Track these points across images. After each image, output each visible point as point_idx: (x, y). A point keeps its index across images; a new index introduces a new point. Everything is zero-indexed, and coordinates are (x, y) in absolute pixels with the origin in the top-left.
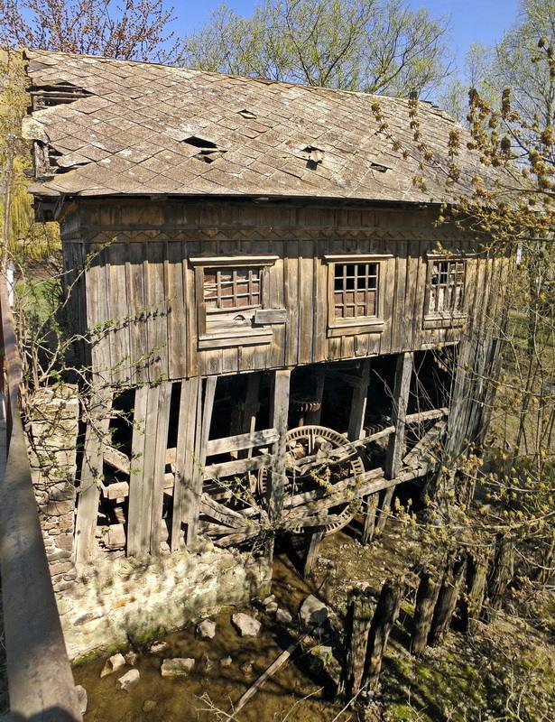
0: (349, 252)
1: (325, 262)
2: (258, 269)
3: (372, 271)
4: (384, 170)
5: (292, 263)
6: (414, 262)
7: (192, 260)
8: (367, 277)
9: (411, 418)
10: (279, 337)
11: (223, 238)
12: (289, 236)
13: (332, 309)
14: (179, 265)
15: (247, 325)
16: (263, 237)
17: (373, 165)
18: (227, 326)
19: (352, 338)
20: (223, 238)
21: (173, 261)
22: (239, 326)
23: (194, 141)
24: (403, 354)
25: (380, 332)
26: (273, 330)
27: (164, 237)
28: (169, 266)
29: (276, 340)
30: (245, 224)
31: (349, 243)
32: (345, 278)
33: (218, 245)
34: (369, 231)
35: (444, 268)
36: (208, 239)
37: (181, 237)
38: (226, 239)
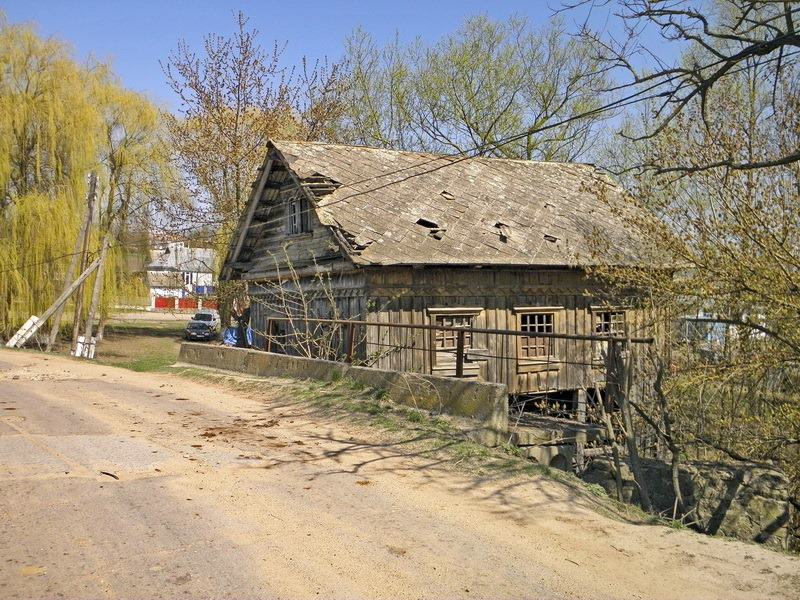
0: (530, 304)
1: (514, 313)
2: (468, 318)
3: (548, 321)
4: (554, 241)
5: (492, 313)
6: (580, 313)
7: (430, 309)
8: (544, 325)
9: (589, 452)
11: (447, 294)
13: (520, 350)
14: (420, 313)
17: (546, 236)
19: (535, 375)
20: (447, 294)
21: (417, 311)
23: (422, 222)
24: (577, 390)
25: (557, 370)
28: (415, 313)
29: (481, 374)
30: (461, 283)
31: (530, 299)
32: (528, 325)
34: (545, 288)
35: (607, 318)
37: (422, 293)
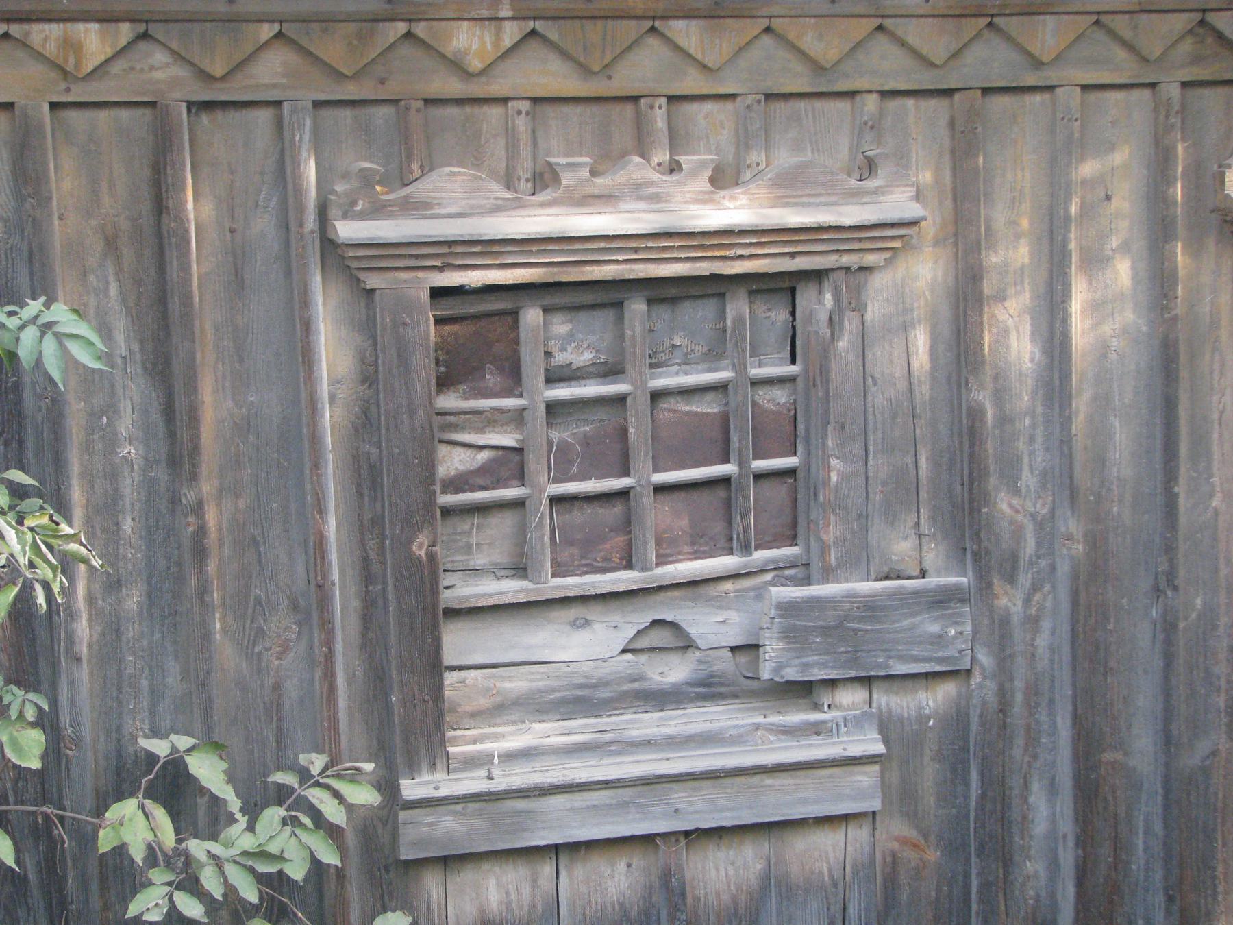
2: (784, 287)
10: (929, 774)
11: (550, 75)
12: (990, 60)
15: (708, 689)
16: (818, 68)
18: (582, 700)
20: (550, 75)
22: (661, 699)
26: (886, 725)
27: (159, 70)
33: (522, 124)
36: (454, 87)
38: (573, 85)
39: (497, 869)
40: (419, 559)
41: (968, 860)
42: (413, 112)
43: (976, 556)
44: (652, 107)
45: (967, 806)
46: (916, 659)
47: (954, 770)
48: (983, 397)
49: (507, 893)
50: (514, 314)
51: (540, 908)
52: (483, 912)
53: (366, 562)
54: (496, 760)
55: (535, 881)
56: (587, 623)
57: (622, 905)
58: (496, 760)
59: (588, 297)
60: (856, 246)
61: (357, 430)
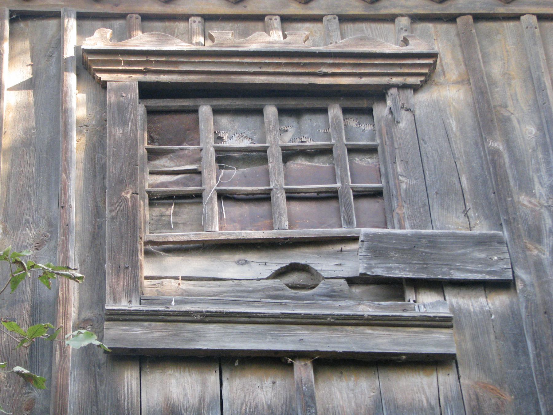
39: (177, 374)
40: (126, 199)
41: (537, 403)
42: (134, 18)
43: (508, 222)
44: (271, 19)
45: (530, 368)
46: (471, 271)
47: (515, 345)
48: (498, 145)
49: (184, 389)
50: (195, 111)
51: (208, 400)
52: (167, 400)
53: (97, 207)
54: (173, 303)
55: (204, 384)
56: (247, 262)
57: (269, 406)
58: (173, 303)
59: (238, 103)
60: (398, 70)
61: (95, 147)
